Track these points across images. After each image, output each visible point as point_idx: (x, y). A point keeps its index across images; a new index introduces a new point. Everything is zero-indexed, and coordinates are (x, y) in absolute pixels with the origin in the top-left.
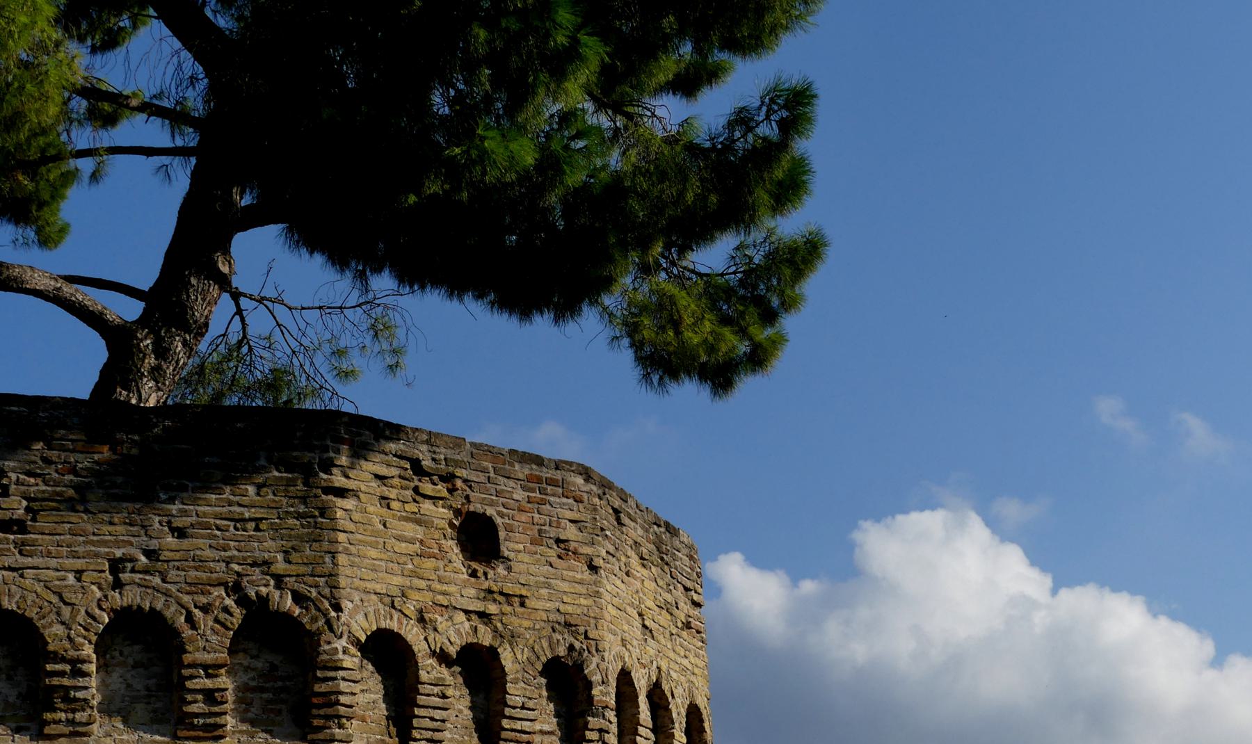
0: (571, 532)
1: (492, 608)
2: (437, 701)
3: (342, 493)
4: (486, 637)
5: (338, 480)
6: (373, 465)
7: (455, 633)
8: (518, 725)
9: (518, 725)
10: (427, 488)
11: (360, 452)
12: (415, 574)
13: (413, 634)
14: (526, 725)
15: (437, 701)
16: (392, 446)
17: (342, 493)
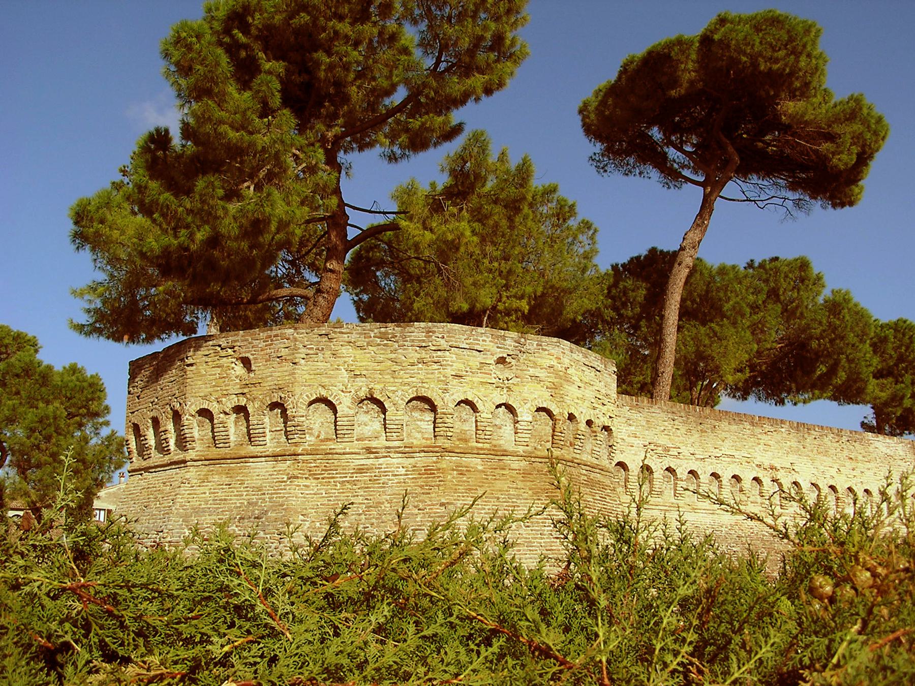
0: (284, 352)
1: (246, 391)
2: (223, 429)
3: (192, 365)
4: (243, 402)
5: (188, 361)
6: (203, 351)
7: (230, 403)
8: (257, 431)
9: (257, 431)
10: (223, 353)
11: (197, 348)
12: (214, 386)
13: (214, 408)
14: (261, 431)
15: (223, 429)
16: (211, 343)
17: (192, 365)
